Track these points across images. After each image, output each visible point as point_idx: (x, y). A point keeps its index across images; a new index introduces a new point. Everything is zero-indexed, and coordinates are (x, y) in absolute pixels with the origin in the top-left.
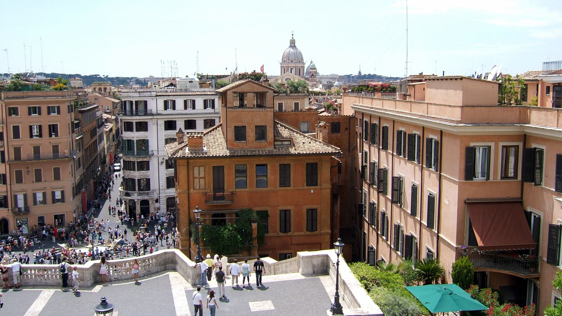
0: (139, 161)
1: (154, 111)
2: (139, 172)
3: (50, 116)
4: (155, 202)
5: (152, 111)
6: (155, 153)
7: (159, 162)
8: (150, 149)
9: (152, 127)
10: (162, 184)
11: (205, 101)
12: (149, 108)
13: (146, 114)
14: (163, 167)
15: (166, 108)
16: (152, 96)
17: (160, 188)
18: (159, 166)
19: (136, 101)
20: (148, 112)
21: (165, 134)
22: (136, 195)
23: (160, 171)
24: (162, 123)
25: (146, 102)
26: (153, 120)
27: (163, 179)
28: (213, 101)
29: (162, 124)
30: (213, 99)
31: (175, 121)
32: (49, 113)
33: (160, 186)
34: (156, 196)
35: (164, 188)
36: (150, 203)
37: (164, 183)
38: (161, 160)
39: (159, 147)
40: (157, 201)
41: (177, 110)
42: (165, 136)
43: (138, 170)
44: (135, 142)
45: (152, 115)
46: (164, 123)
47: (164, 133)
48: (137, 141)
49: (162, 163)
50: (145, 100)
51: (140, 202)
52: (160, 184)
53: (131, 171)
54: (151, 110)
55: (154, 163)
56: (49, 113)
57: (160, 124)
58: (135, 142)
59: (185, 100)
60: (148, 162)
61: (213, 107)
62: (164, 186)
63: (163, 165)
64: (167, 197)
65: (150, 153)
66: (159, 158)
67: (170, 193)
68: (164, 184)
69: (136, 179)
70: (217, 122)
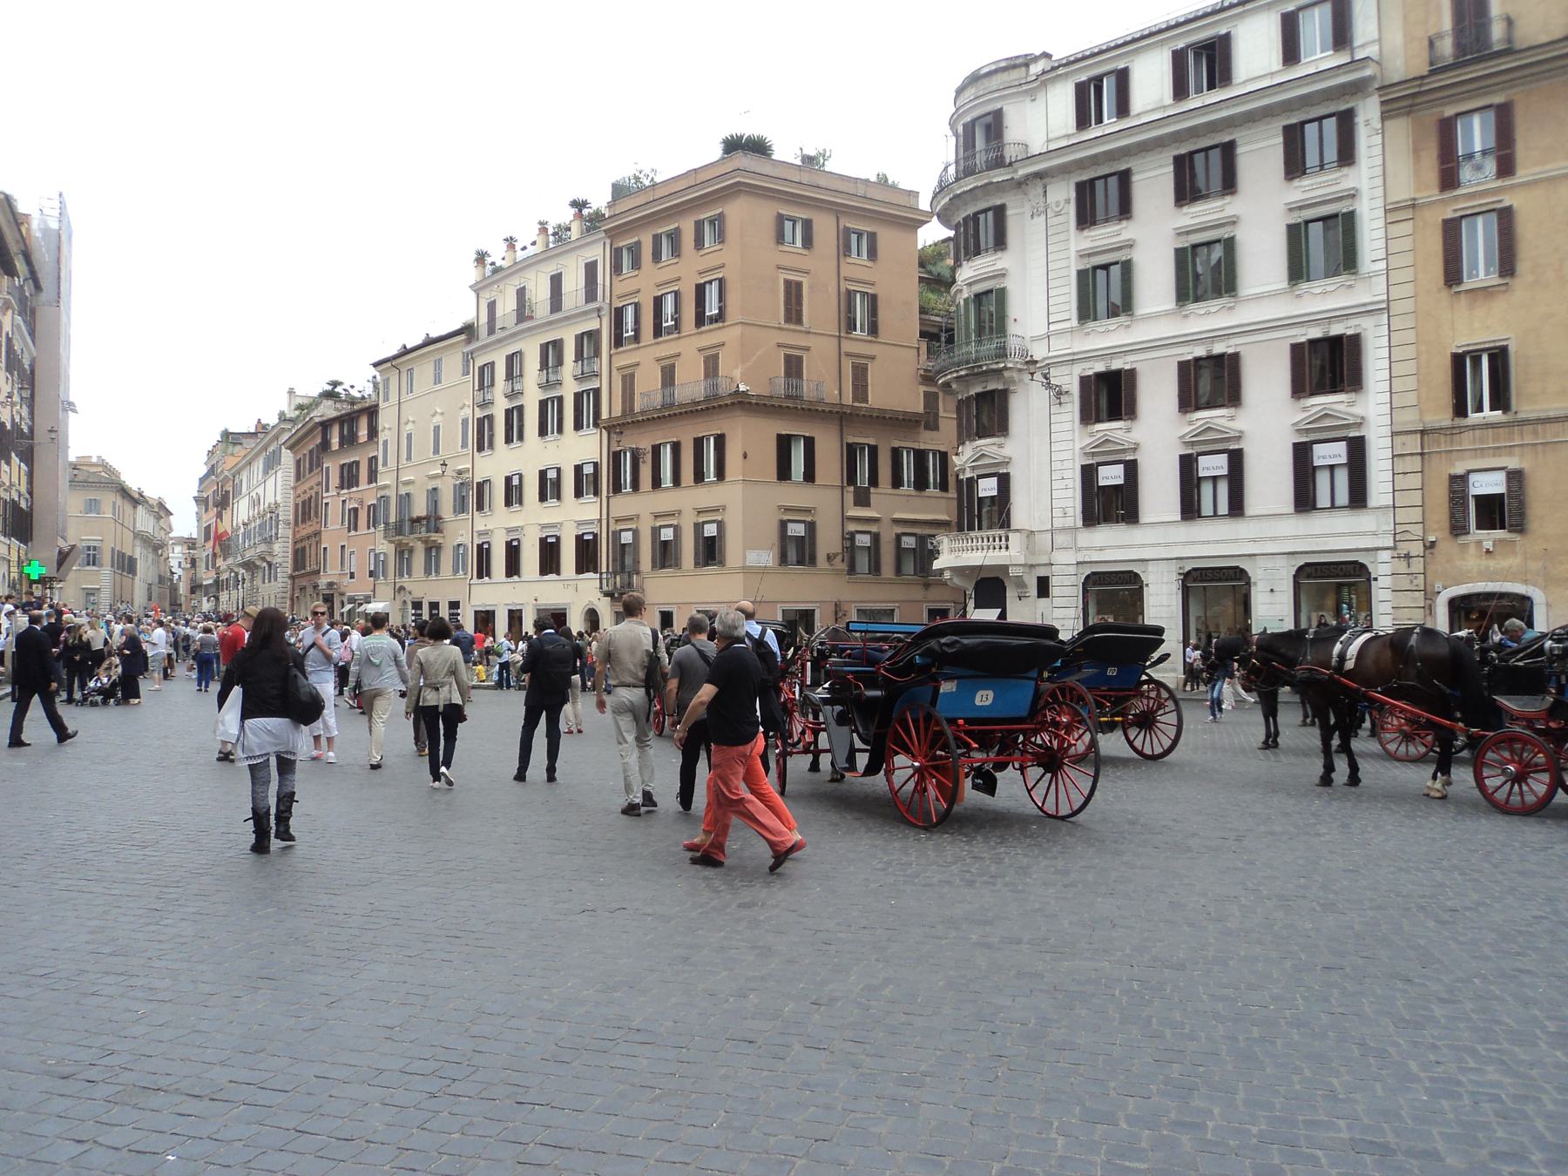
14: (1067, 417)
27: (1068, 474)
35: (1069, 522)
37: (1070, 498)
62: (1070, 512)
63: (1068, 407)
67: (1101, 549)
68: (1070, 503)
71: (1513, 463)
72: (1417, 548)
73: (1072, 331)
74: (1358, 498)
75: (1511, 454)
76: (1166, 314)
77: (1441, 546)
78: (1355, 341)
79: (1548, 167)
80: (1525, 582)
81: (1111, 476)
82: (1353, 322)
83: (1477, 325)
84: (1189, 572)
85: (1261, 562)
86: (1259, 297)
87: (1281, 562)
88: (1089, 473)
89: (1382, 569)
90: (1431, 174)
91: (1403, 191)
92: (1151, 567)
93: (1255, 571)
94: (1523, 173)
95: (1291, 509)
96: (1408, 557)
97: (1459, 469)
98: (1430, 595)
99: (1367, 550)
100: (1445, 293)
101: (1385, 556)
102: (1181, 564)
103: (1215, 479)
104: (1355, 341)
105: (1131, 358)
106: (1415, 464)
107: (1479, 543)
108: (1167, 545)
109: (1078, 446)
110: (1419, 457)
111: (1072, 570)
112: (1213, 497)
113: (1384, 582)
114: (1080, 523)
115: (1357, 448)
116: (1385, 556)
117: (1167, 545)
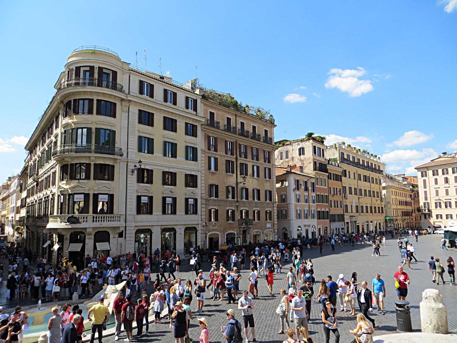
0: (97, 163)
4: (117, 236)
7: (129, 170)
17: (128, 213)
18: (129, 176)
22: (90, 219)
24: (134, 111)
26: (124, 103)
30: (195, 98)
33: (128, 209)
34: (121, 224)
36: (111, 236)
38: (131, 167)
39: (129, 147)
40: (121, 235)
43: (95, 178)
51: (95, 235)
55: (120, 172)
62: (133, 210)
64: (137, 228)
66: (129, 164)
69: (91, 193)
71: (217, 208)
72: (204, 224)
74: (195, 212)
75: (216, 206)
77: (207, 224)
78: (197, 176)
79: (221, 153)
80: (218, 231)
81: (145, 200)
83: (212, 179)
84: (163, 229)
88: (139, 198)
89: (199, 228)
90: (207, 146)
91: (203, 148)
93: (177, 228)
94: (218, 153)
96: (203, 226)
97: (210, 208)
98: (206, 234)
99: (197, 224)
100: (208, 171)
101: (200, 226)
102: (162, 227)
103: (168, 204)
106: (204, 206)
107: (212, 224)
109: (135, 189)
110: (205, 205)
111: (133, 228)
112: (169, 210)
114: (135, 213)
115: (196, 200)
116: (200, 226)
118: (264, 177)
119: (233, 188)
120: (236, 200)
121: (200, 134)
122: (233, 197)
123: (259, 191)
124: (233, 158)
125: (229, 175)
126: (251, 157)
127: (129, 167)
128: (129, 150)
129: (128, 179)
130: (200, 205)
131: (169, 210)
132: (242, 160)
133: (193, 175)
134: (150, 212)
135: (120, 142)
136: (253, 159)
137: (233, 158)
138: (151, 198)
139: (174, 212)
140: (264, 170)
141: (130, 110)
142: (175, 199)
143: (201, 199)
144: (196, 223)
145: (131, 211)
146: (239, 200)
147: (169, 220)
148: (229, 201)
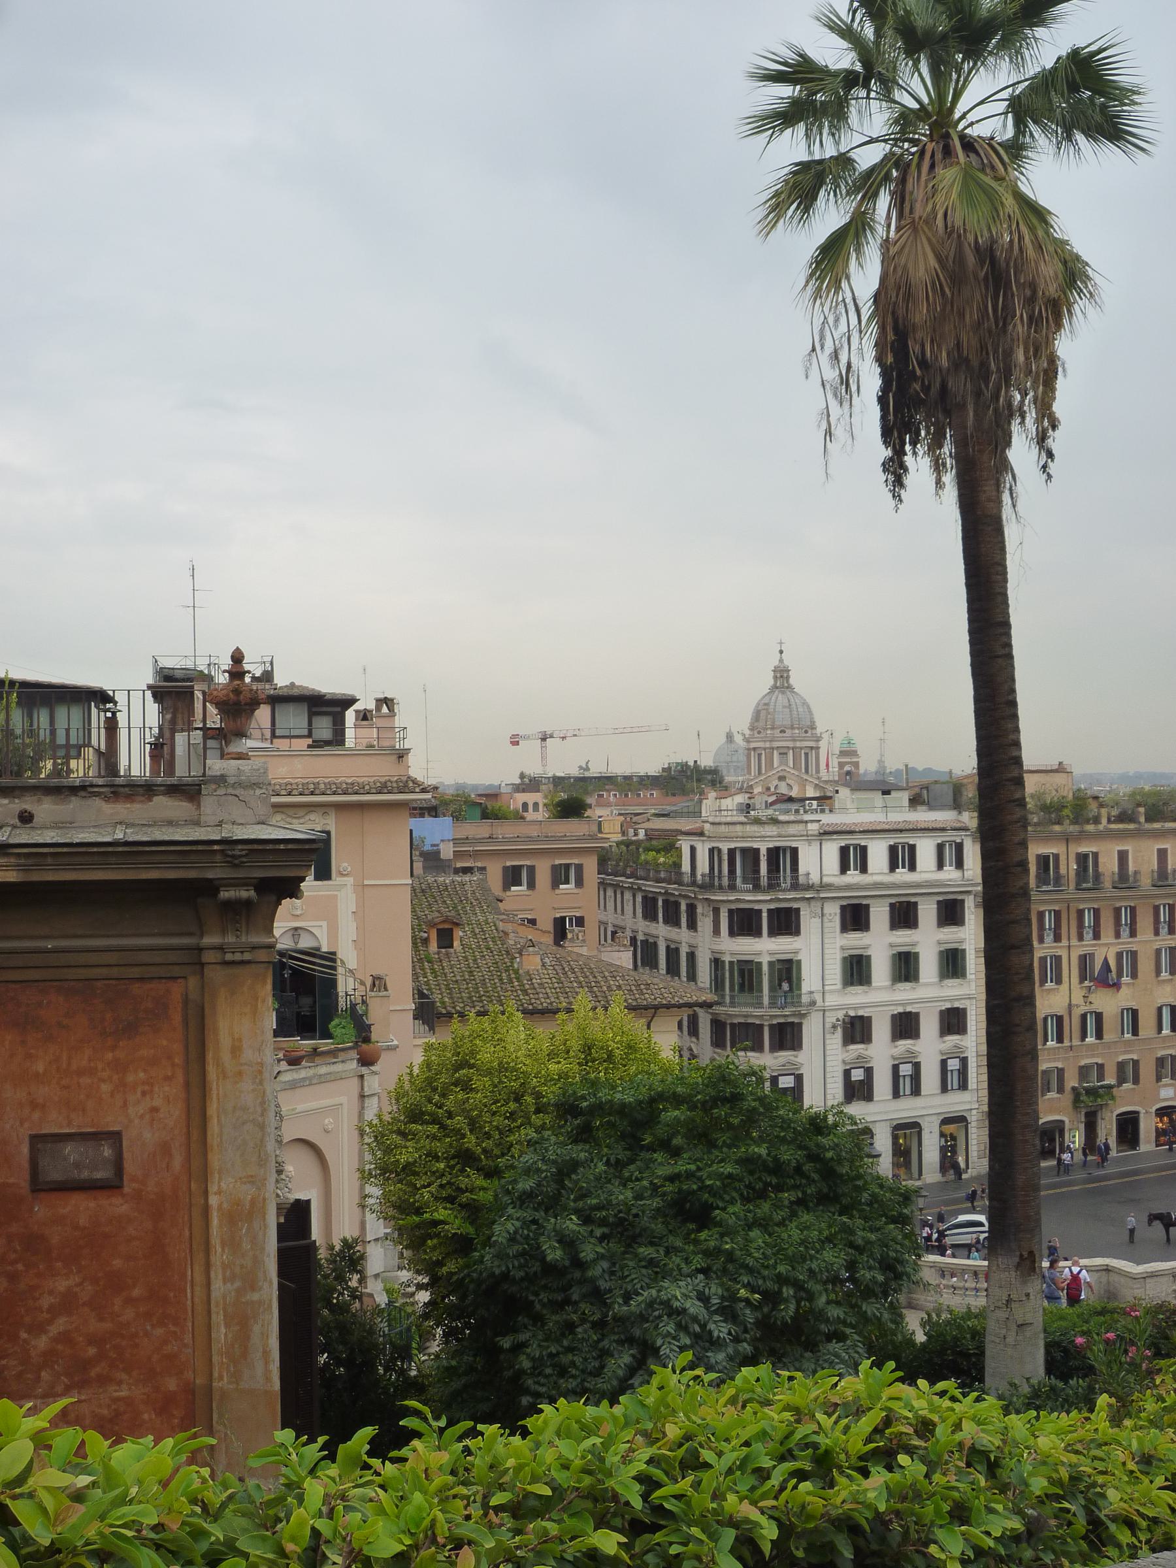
1: (815, 878)
2: (776, 1054)
3: (557, 891)
5: (811, 876)
6: (818, 998)
7: (828, 1025)
8: (805, 987)
9: (809, 921)
10: (833, 1091)
11: (940, 848)
12: (802, 868)
13: (795, 886)
15: (844, 868)
16: (810, 833)
18: (828, 1036)
19: (769, 850)
20: (802, 880)
21: (841, 943)
23: (828, 1053)
24: (833, 911)
25: (795, 852)
26: (813, 903)
27: (835, 1074)
28: (959, 848)
29: (836, 914)
30: (958, 841)
31: (867, 907)
32: (555, 884)
33: (828, 1097)
41: (872, 874)
42: (843, 949)
43: (773, 1049)
44: (765, 968)
45: (809, 887)
46: (838, 911)
47: (838, 939)
48: (771, 964)
49: (834, 1027)
50: (794, 845)
52: (828, 1091)
53: (749, 1054)
54: (809, 874)
55: (811, 1030)
56: (555, 884)
57: (830, 914)
58: (765, 968)
59: (890, 846)
60: (800, 1025)
61: (959, 864)
65: (805, 999)
66: (827, 1014)
70: (969, 908)
73: (838, 991)
74: (963, 1086)
76: (885, 988)
78: (964, 1010)
81: (857, 1075)
82: (963, 1001)
85: (927, 1118)
86: (926, 985)
87: (934, 1118)
88: (847, 1073)
92: (877, 1124)
95: (939, 1091)
103: (904, 1076)
104: (964, 1010)
105: (867, 1010)
108: (886, 1113)
109: (840, 1058)
112: (906, 1086)
113: (974, 1124)
115: (964, 1061)
116: (974, 1112)
117: (886, 1113)
118: (1154, 974)
119: (1060, 1019)
120: (1066, 1043)
121: (973, 917)
122: (1060, 1039)
123: (1135, 1013)
124: (1060, 947)
125: (1049, 991)
126: (1111, 932)
127: (827, 1020)
128: (827, 988)
129: (828, 1042)
130: (975, 1070)
131: (906, 1086)
132: (1087, 946)
133: (958, 1009)
134: (868, 1096)
135: (810, 981)
136: (1118, 935)
137: (1060, 947)
138: (869, 1071)
139: (916, 1091)
140: (1153, 957)
141: (825, 912)
142: (917, 1066)
143: (978, 1056)
144: (968, 1107)
145: (834, 1098)
146: (1076, 1042)
147: (907, 1109)
148: (1049, 1049)
